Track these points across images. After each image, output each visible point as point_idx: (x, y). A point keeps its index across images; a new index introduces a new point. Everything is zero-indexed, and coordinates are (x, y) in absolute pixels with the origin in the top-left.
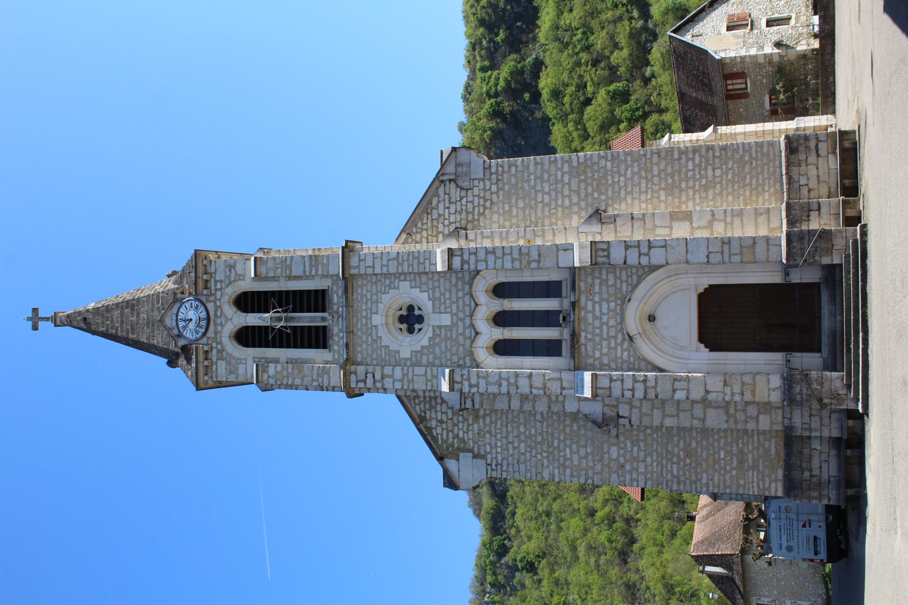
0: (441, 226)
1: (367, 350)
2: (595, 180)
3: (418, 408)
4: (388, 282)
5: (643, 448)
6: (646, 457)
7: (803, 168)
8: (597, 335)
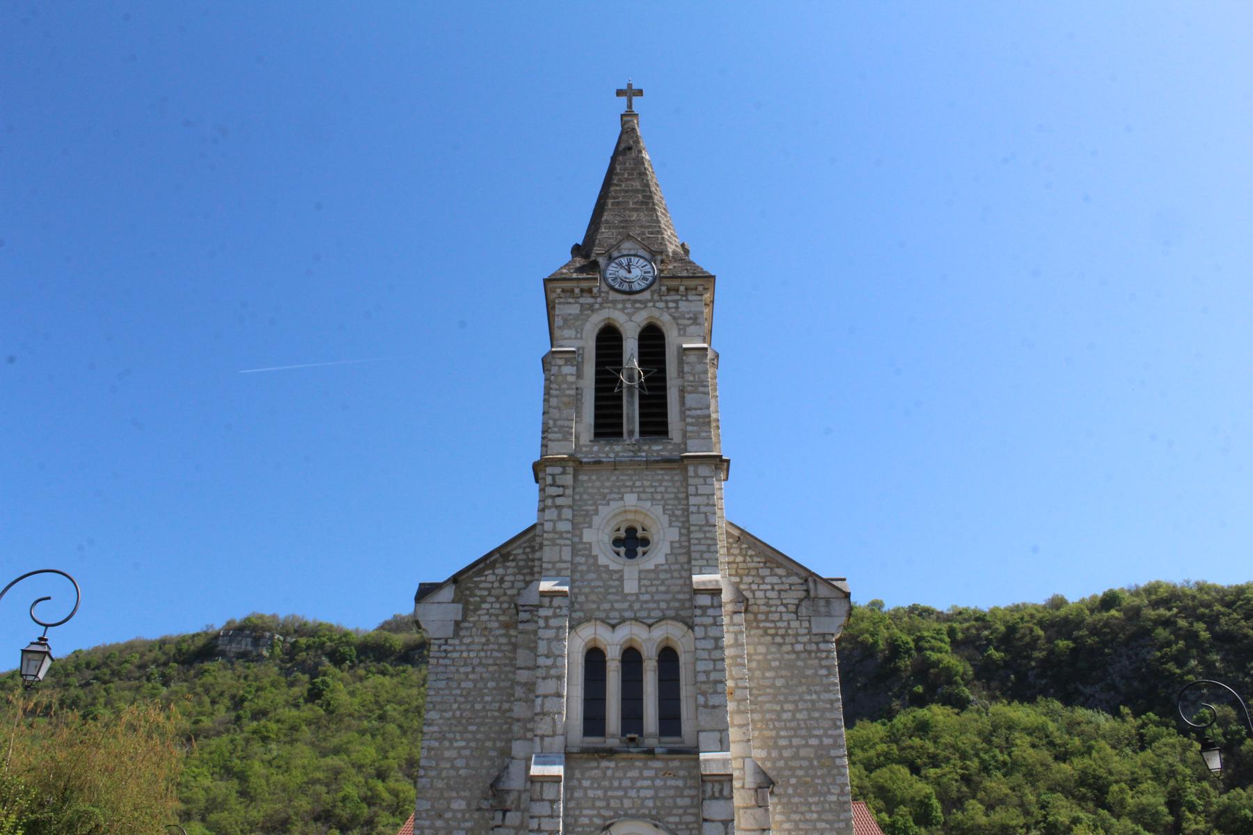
0: (750, 579)
1: (593, 487)
2: (813, 780)
3: (520, 551)
4: (678, 513)
8: (611, 784)
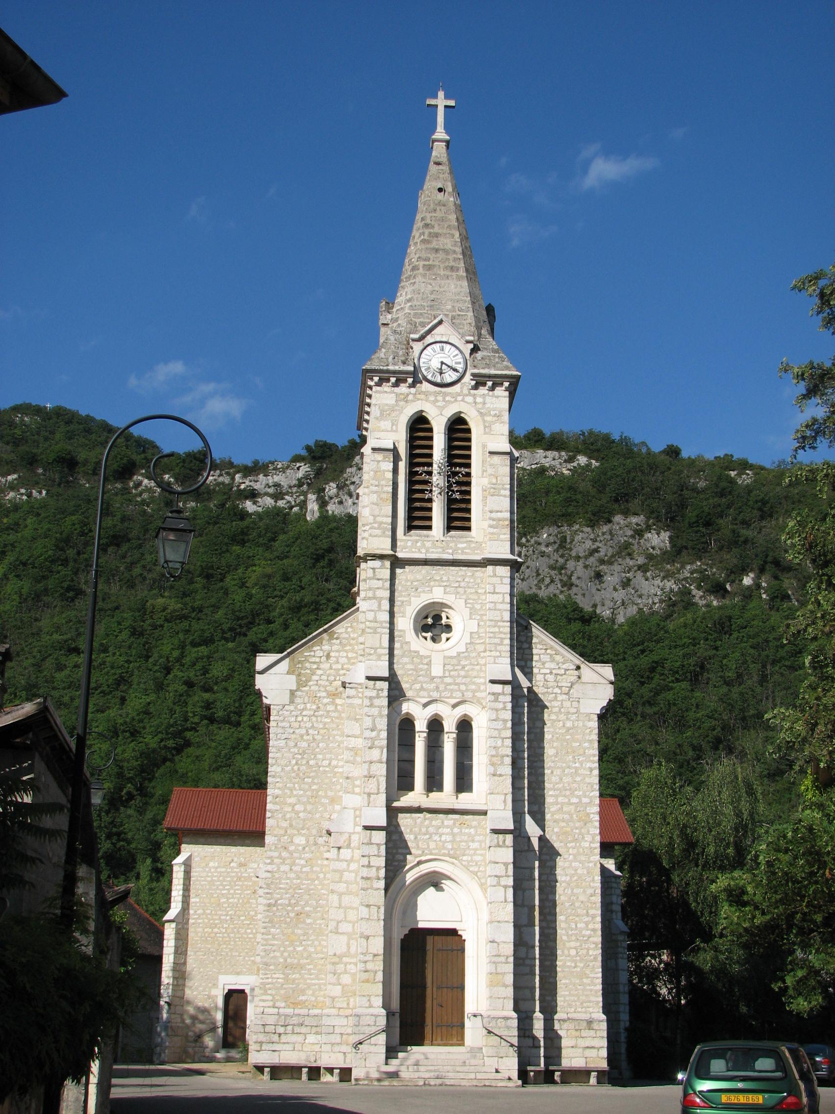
2: (572, 830)
3: (343, 630)
5: (304, 869)
6: (296, 872)
7: (574, 1033)
8: (420, 830)
